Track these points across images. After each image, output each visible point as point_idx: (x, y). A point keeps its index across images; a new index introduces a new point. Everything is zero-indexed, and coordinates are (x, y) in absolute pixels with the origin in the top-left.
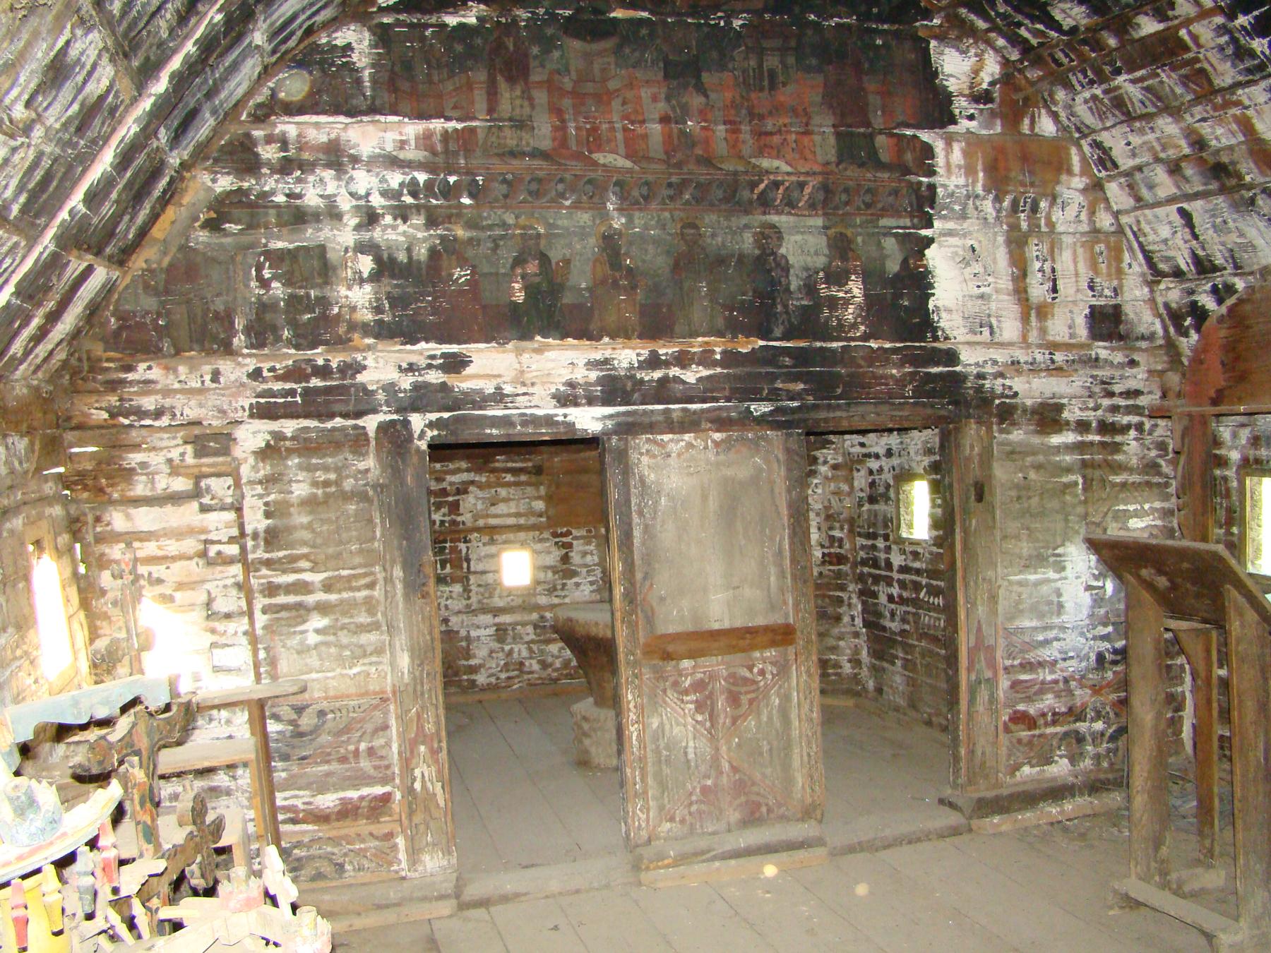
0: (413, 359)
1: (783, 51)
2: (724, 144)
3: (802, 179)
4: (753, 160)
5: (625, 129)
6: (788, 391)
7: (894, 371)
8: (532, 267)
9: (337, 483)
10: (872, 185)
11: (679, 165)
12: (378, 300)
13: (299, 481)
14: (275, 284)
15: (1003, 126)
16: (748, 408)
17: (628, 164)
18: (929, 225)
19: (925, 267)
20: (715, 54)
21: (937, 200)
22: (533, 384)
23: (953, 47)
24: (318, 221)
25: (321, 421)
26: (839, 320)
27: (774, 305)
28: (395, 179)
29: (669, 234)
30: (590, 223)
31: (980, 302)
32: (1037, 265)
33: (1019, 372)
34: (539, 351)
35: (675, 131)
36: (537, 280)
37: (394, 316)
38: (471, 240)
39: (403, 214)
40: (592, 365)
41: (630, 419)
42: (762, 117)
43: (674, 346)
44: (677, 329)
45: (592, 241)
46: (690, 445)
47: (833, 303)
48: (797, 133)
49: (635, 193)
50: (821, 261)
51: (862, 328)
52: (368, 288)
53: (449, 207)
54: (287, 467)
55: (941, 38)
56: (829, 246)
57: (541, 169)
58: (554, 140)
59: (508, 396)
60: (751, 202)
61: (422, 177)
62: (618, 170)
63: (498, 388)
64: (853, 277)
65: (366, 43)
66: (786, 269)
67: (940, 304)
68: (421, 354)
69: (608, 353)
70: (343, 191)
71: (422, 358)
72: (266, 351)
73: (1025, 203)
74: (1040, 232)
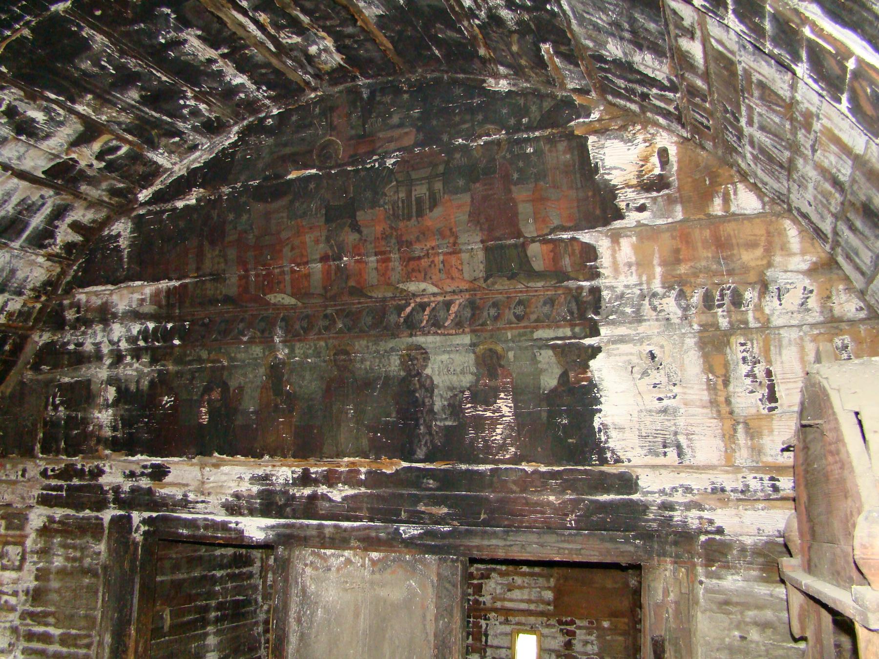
0: (134, 467)
1: (430, 179)
2: (374, 274)
3: (448, 298)
4: (401, 286)
5: (293, 271)
6: (431, 515)
7: (552, 498)
8: (215, 395)
9: (80, 560)
10: (523, 296)
11: (333, 298)
12: (116, 420)
13: (58, 555)
14: (61, 408)
15: (684, 214)
16: (397, 529)
17: (293, 301)
18: (596, 333)
19: (590, 380)
20: (369, 194)
21: (603, 304)
22: (209, 494)
23: (615, 138)
24: (90, 362)
25: (77, 511)
26: (486, 441)
27: (417, 425)
28: (136, 328)
29: (325, 361)
30: (261, 355)
31: (662, 417)
32: (744, 369)
33: (725, 502)
34: (216, 466)
35: (333, 267)
36: (218, 405)
37: (124, 434)
38: (177, 372)
39: (137, 354)
40: (255, 479)
41: (288, 531)
42: (409, 244)
43: (325, 465)
44: (325, 450)
45: (262, 370)
46: (348, 561)
47: (479, 423)
48: (445, 254)
49: (297, 326)
50: (467, 380)
51: (513, 449)
52: (110, 411)
53: (166, 347)
54: (53, 543)
55: (602, 131)
56: (477, 364)
57: (227, 312)
58: (239, 286)
59: (191, 502)
60: (397, 325)
61: (151, 325)
62: (285, 307)
63: (185, 495)
64: (502, 395)
65: (129, 230)
66: (430, 389)
67: (608, 421)
68: (138, 464)
69: (268, 470)
70: (105, 339)
71: (138, 467)
72: (51, 456)
73: (722, 296)
74: (747, 328)
